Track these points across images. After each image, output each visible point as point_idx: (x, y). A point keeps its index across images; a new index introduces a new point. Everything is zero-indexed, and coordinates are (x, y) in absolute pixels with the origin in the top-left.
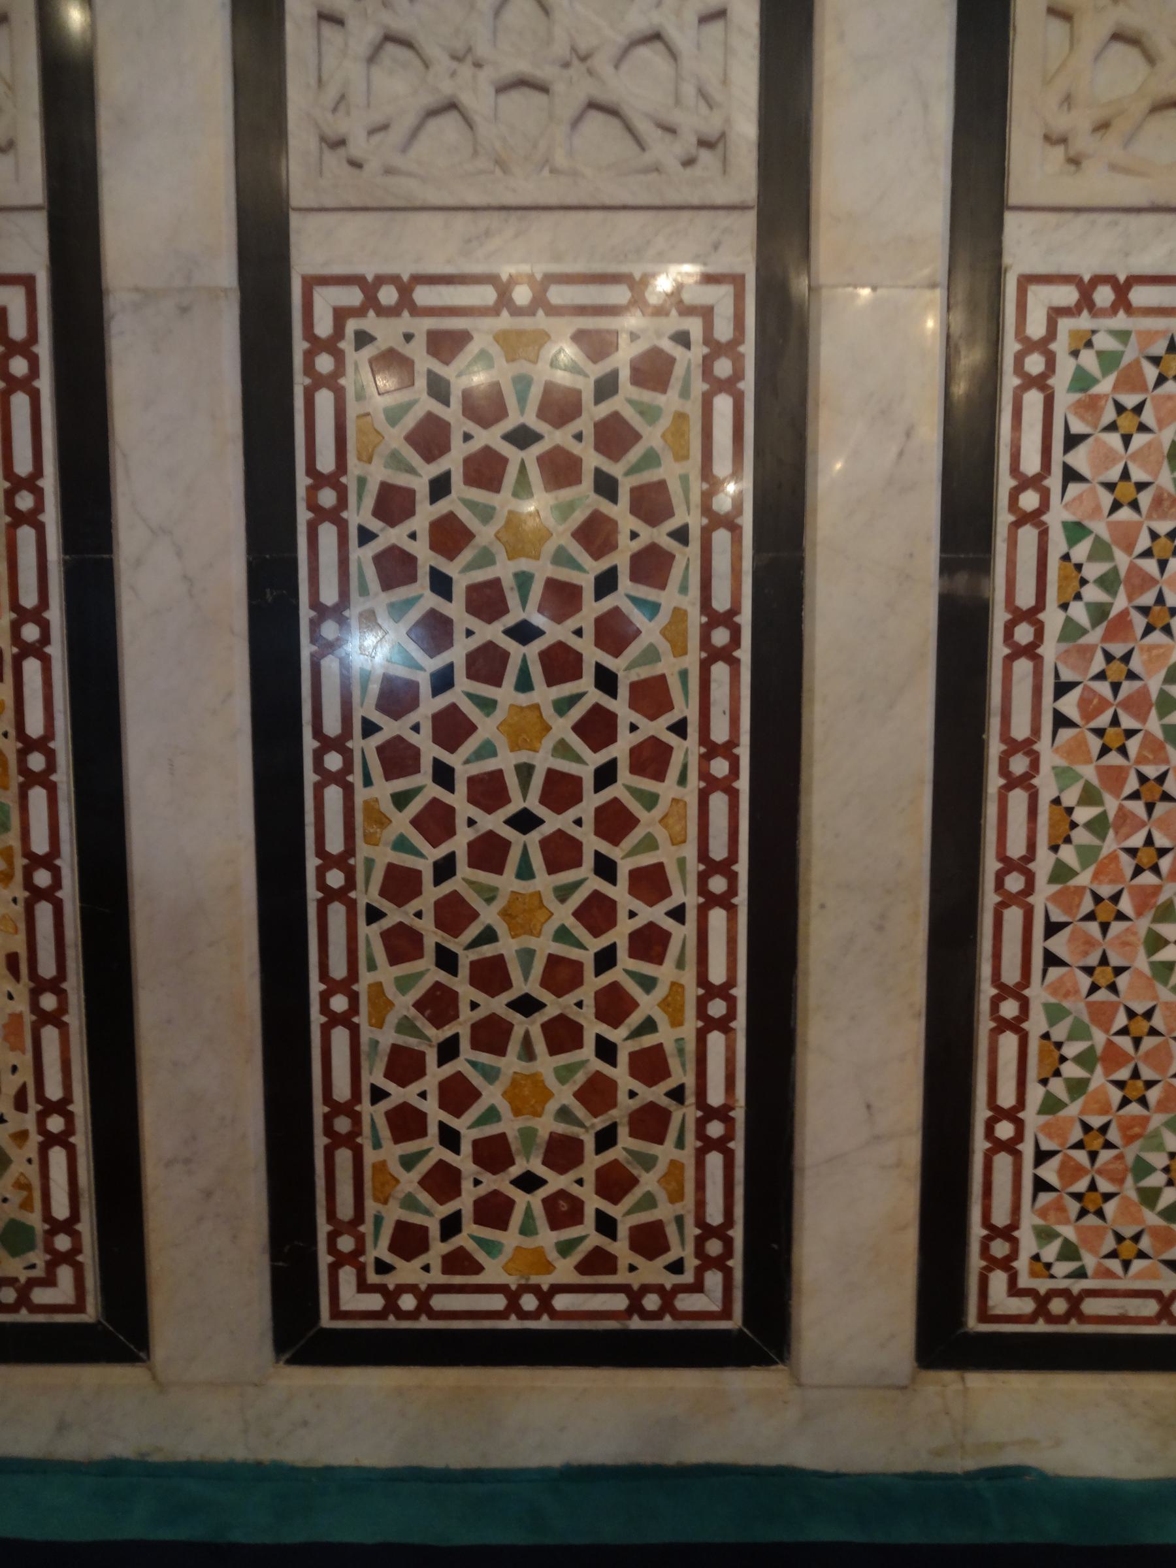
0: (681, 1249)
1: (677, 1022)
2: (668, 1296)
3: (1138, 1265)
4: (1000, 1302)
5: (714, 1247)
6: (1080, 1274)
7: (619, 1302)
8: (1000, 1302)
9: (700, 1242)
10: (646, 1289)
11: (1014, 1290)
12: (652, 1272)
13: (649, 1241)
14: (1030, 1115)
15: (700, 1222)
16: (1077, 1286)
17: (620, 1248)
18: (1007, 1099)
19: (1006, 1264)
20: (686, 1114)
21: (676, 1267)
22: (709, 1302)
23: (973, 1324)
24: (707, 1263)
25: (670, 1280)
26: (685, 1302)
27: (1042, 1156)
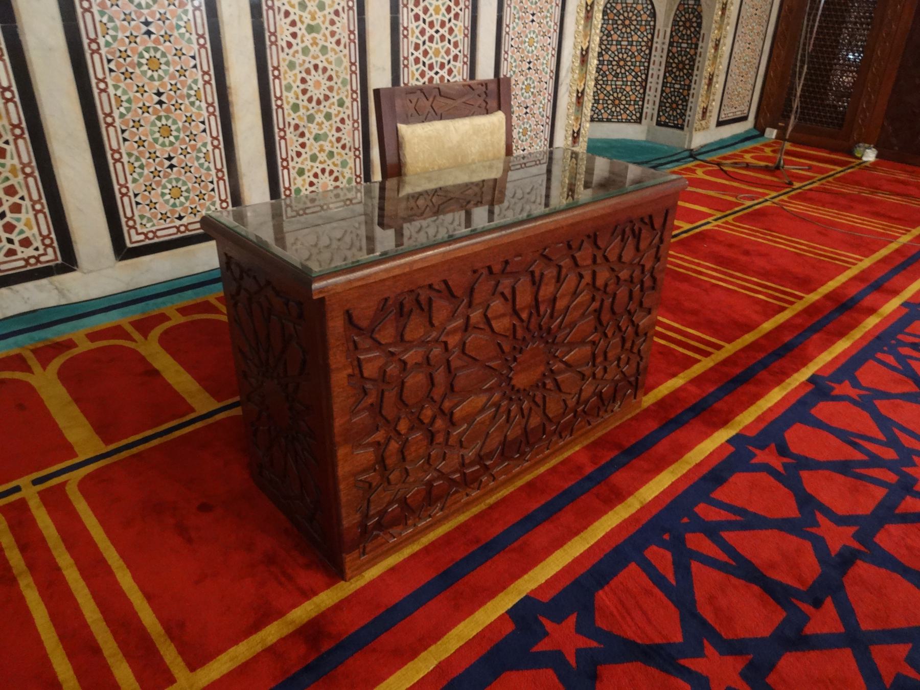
0: (37, 243)
1: (16, 176)
2: (37, 258)
3: (168, 220)
4: (133, 239)
5: (47, 242)
6: (154, 225)
7: (22, 263)
8: (133, 239)
9: (43, 241)
10: (30, 257)
11: (138, 234)
12: (30, 252)
13: (26, 243)
14: (130, 185)
15: (41, 234)
16: (154, 229)
17: (16, 246)
18: (122, 181)
19: (134, 227)
20: (26, 204)
21: (37, 249)
22: (51, 256)
23: (129, 245)
24: (46, 246)
25: (36, 253)
26: (43, 259)
27: (136, 195)
